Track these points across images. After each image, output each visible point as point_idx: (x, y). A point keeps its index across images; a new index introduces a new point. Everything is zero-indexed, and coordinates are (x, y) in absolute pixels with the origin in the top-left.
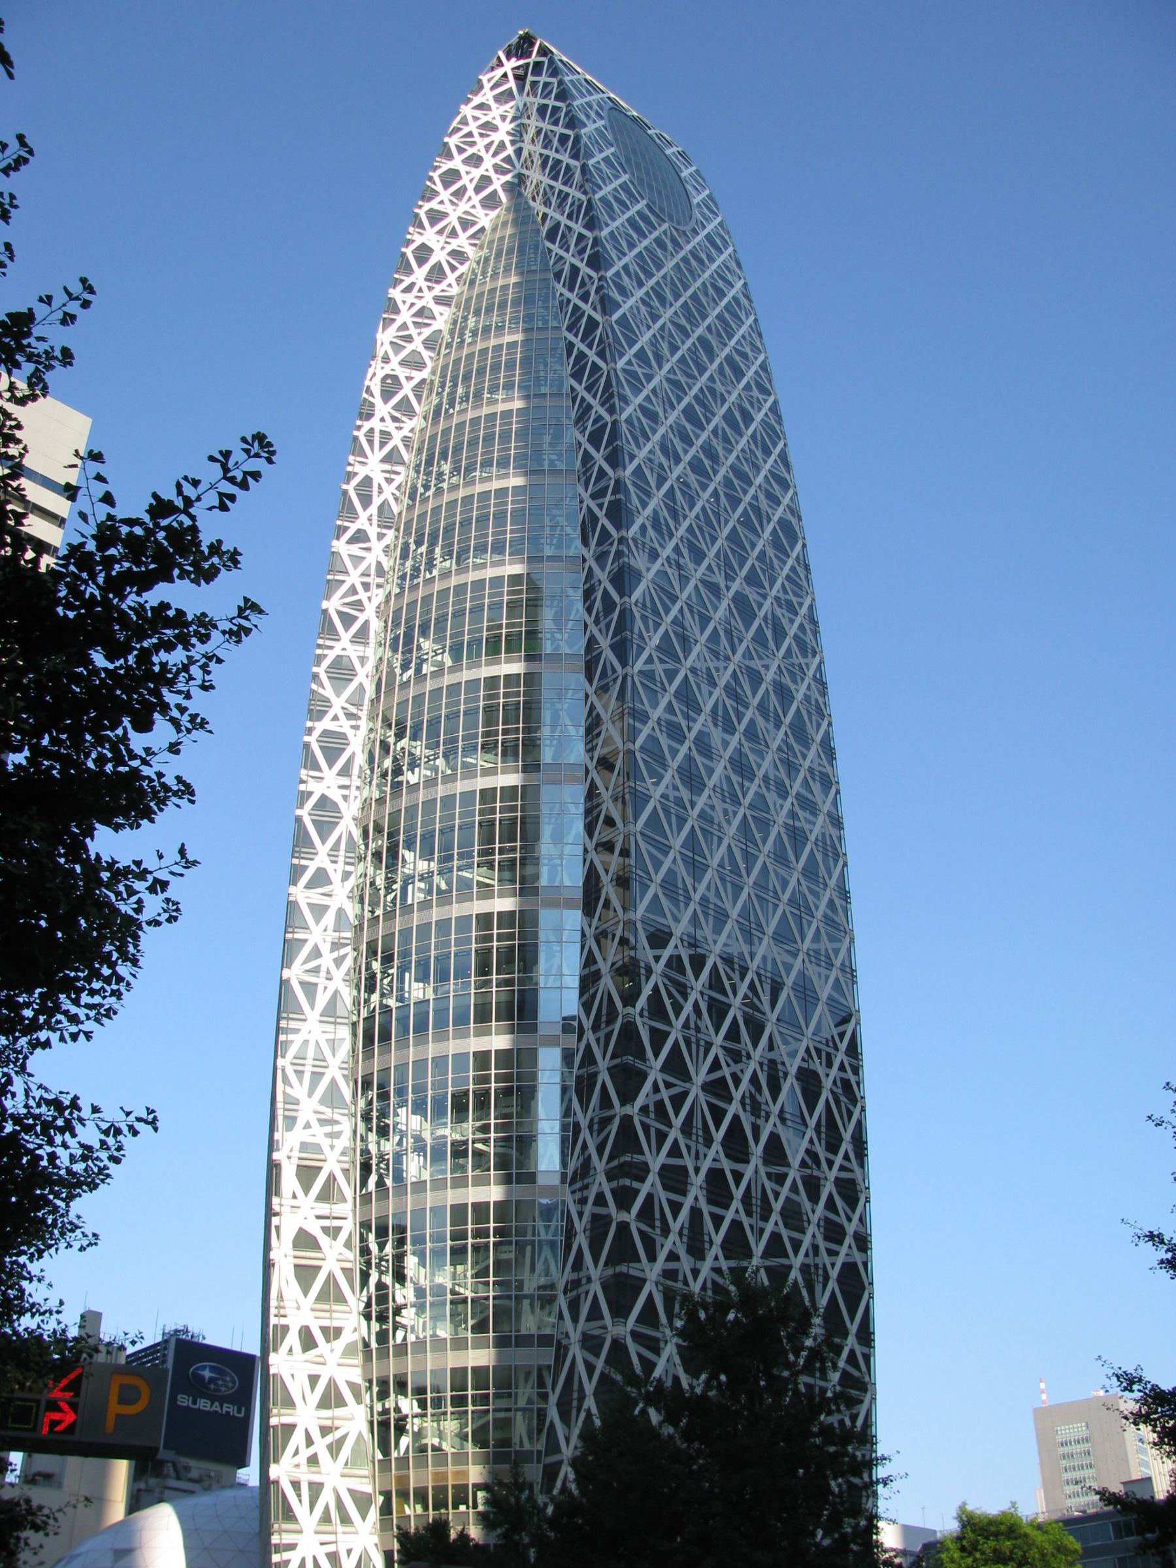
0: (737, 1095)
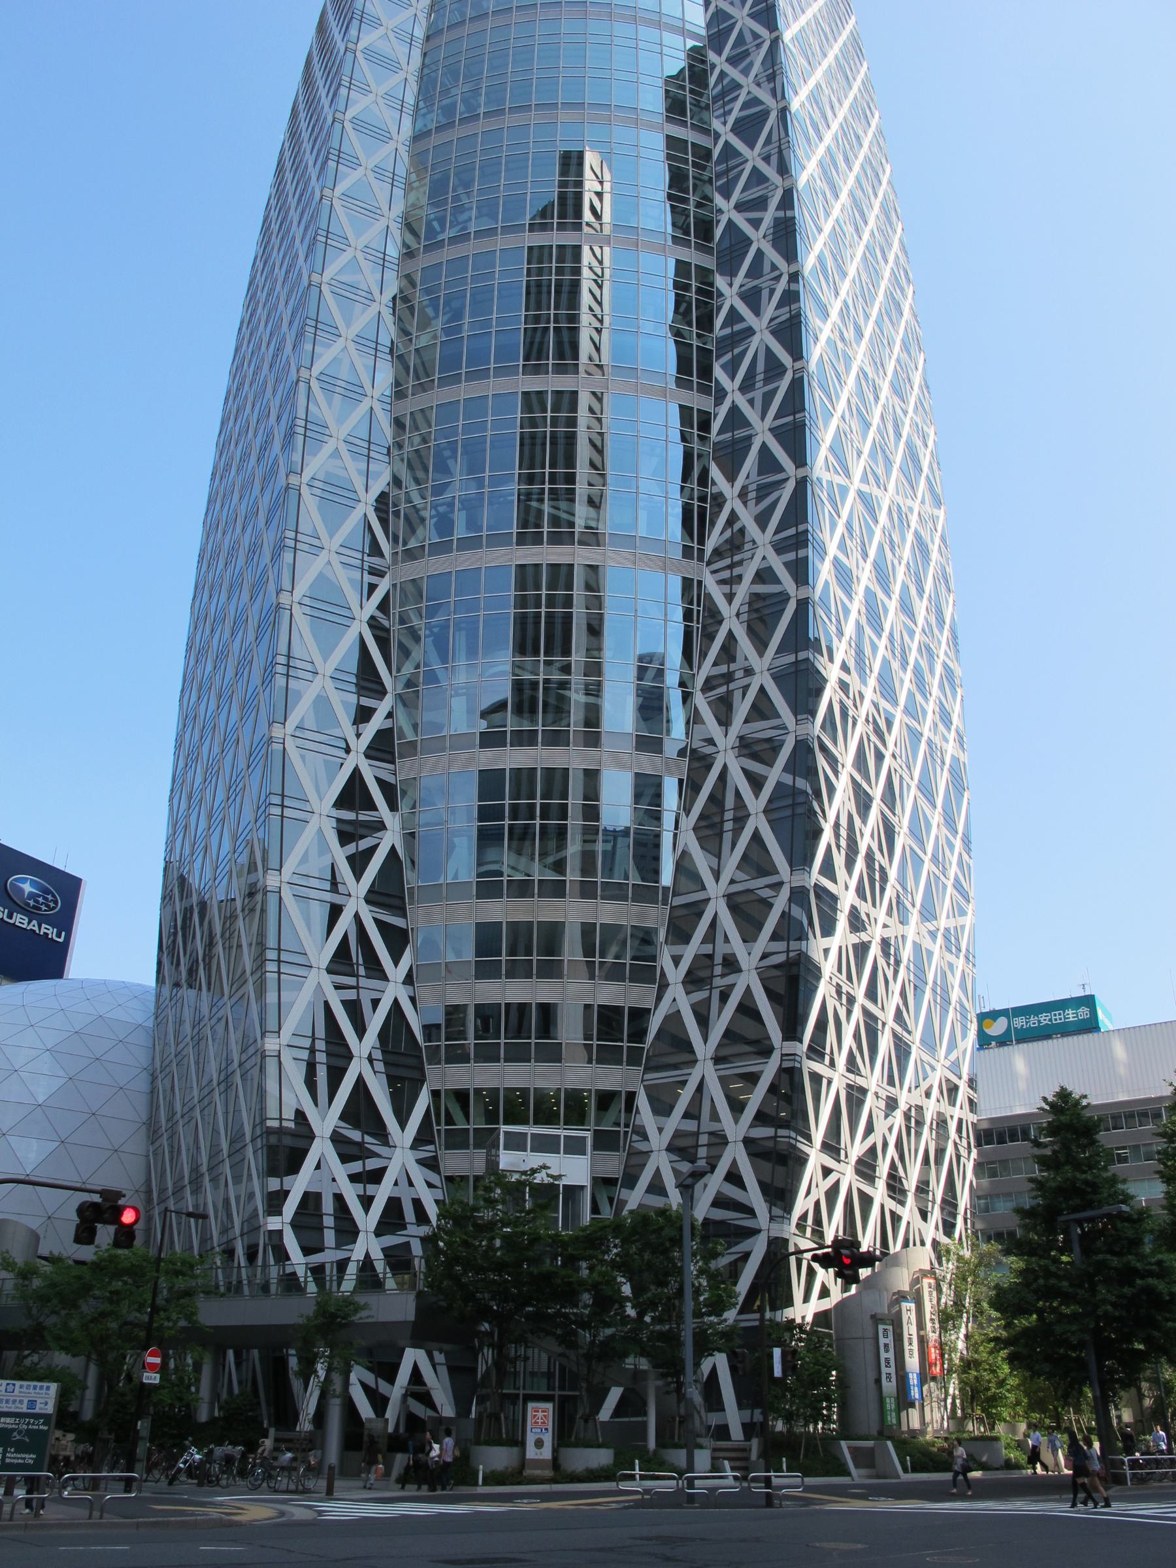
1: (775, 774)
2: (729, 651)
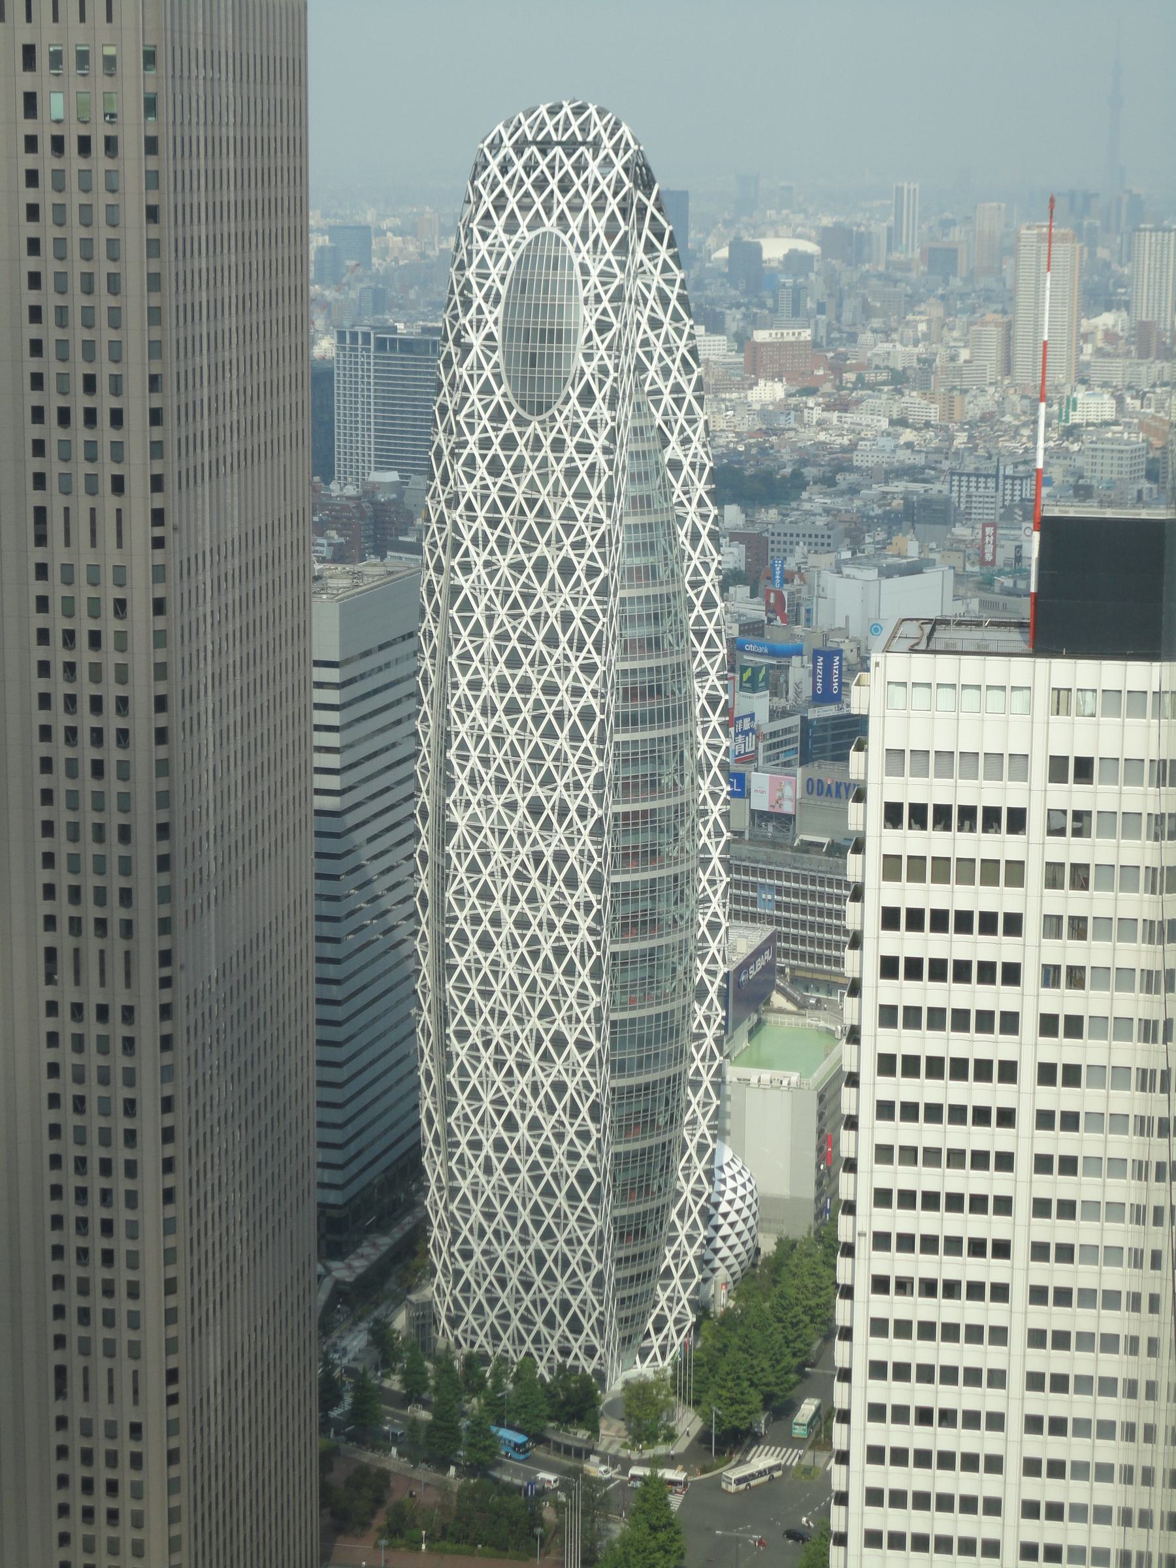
0: (510, 1102)
1: (702, 1202)
2: (690, 1159)
